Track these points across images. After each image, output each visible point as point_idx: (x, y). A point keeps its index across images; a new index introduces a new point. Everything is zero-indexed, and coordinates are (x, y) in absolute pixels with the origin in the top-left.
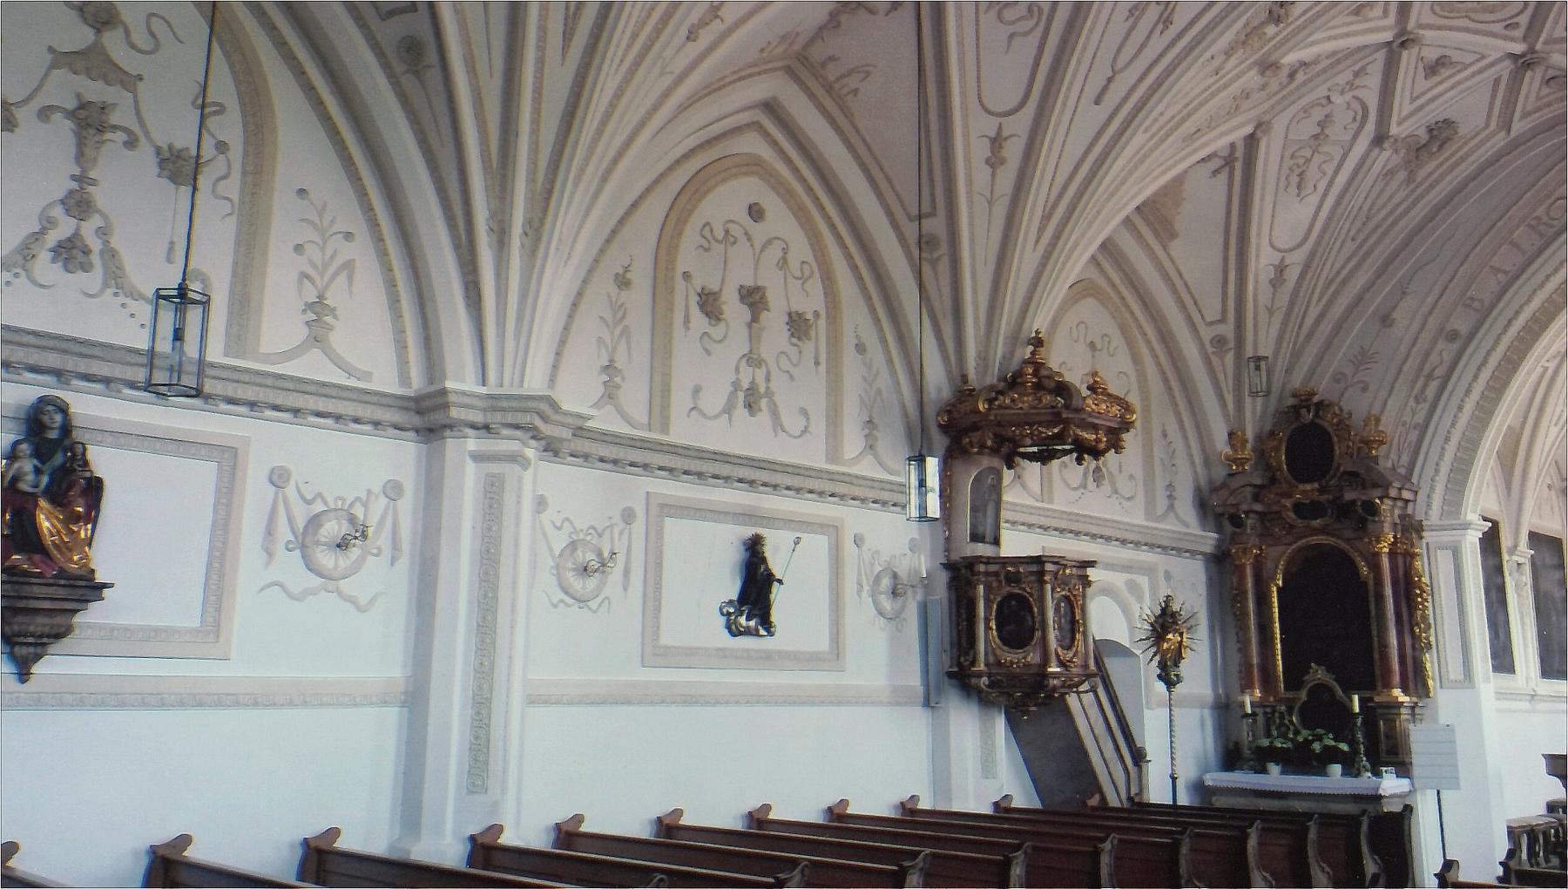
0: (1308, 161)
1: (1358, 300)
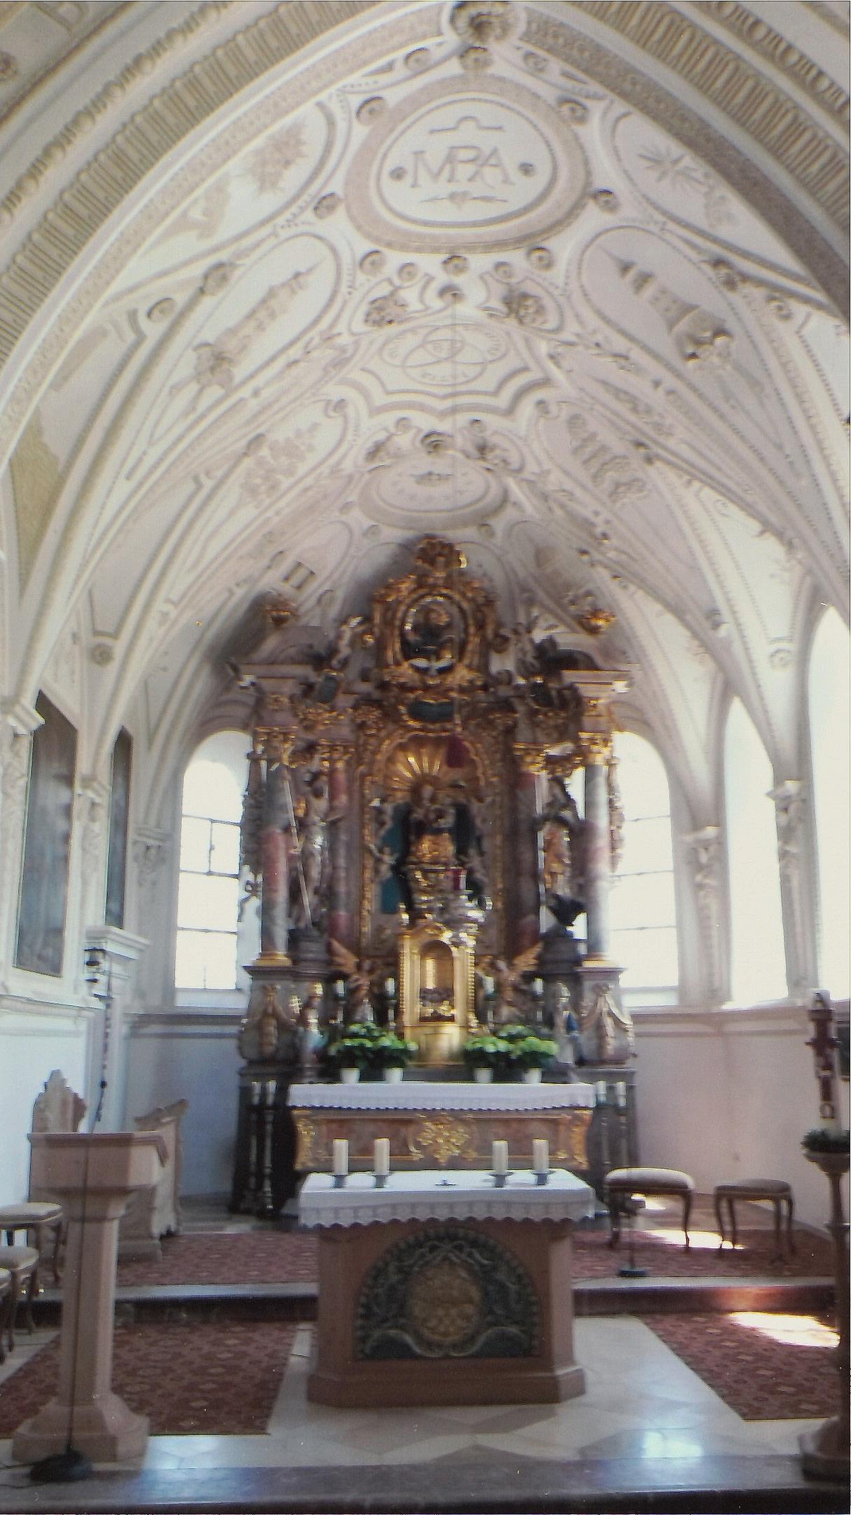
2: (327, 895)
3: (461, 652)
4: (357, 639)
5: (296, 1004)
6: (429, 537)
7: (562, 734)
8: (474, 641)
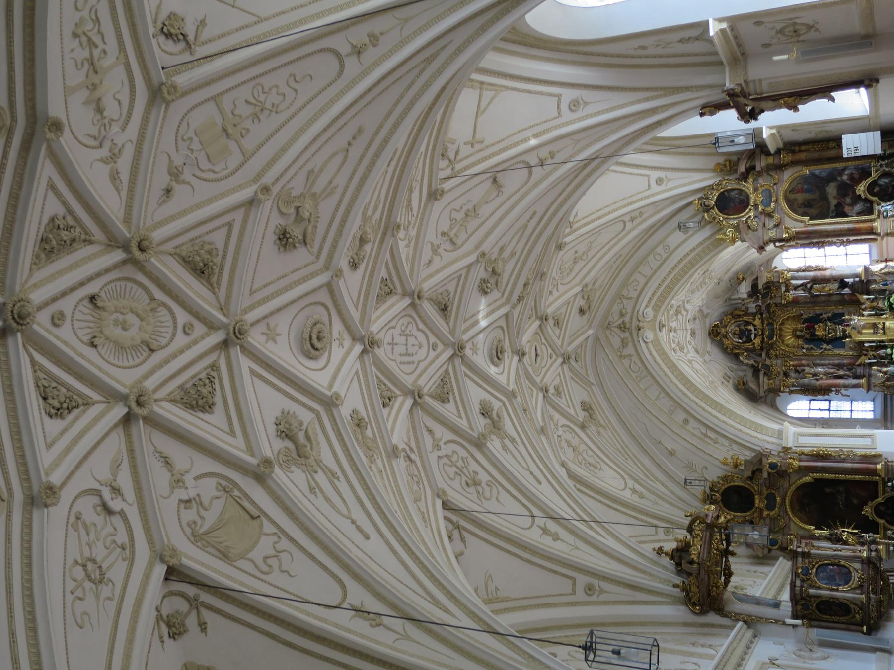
0: (584, 458)
1: (658, 465)
2: (840, 366)
3: (748, 323)
4: (747, 357)
5: (880, 375)
6: (709, 334)
7: (779, 288)
8: (746, 318)
